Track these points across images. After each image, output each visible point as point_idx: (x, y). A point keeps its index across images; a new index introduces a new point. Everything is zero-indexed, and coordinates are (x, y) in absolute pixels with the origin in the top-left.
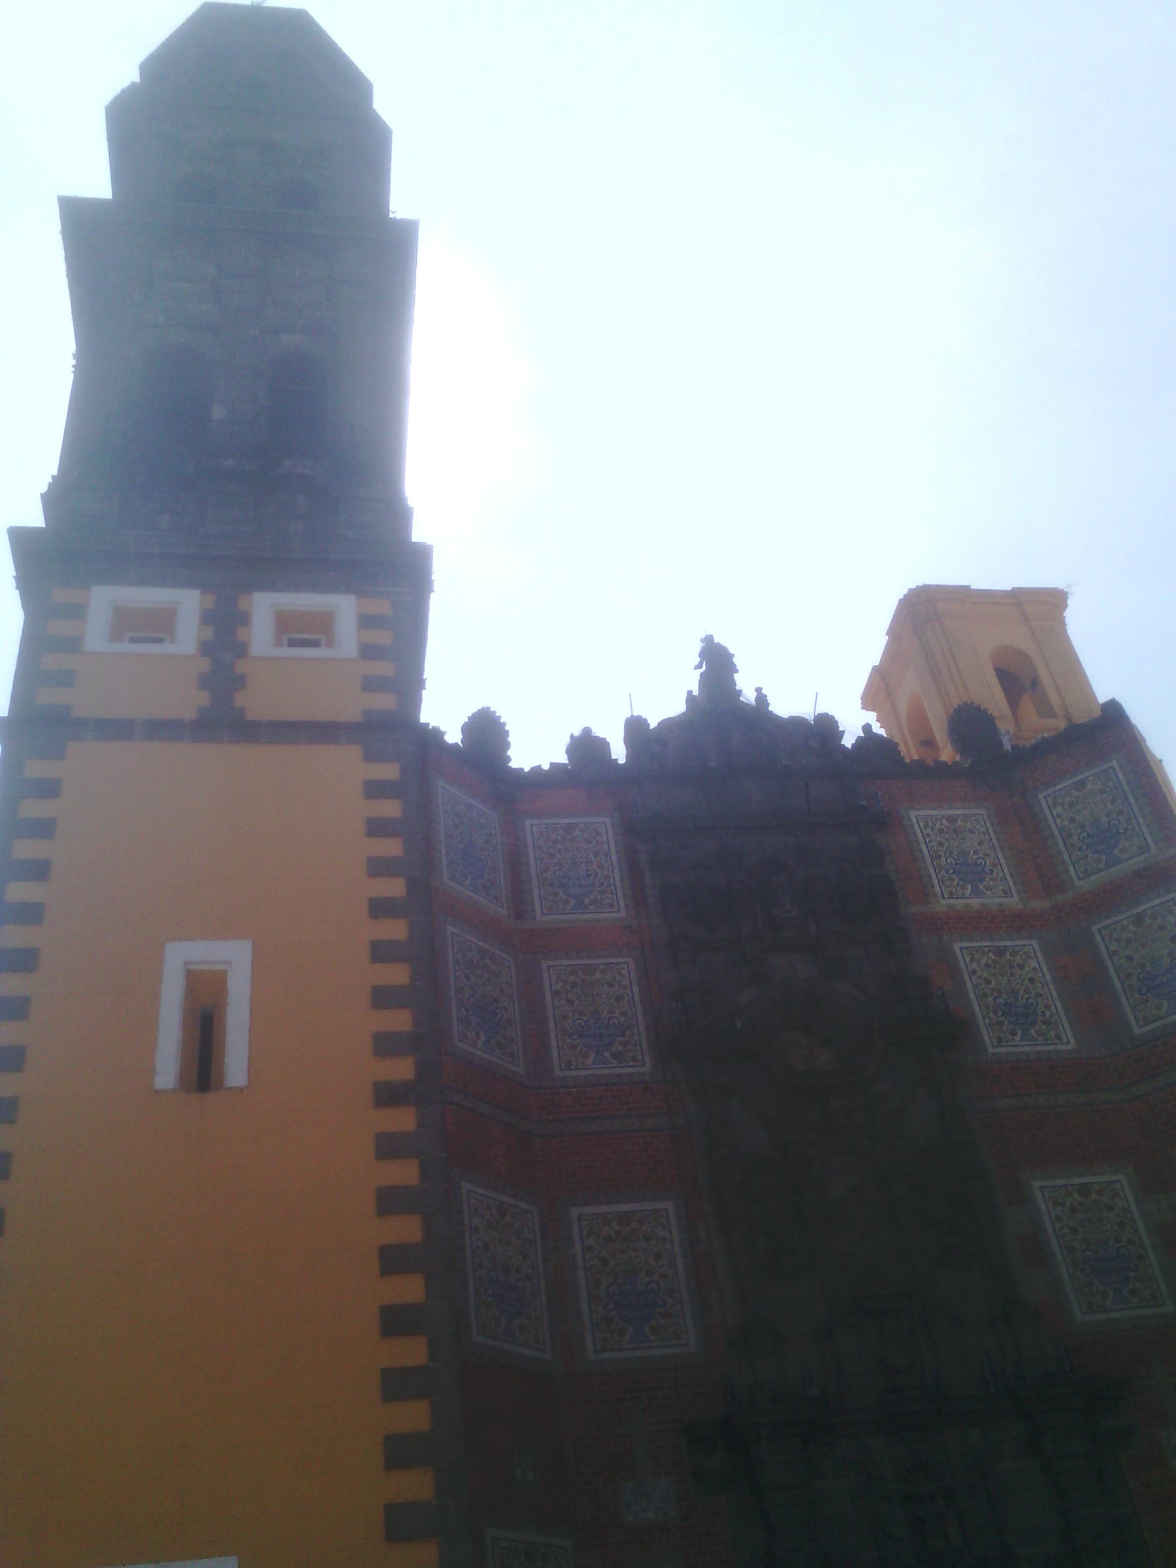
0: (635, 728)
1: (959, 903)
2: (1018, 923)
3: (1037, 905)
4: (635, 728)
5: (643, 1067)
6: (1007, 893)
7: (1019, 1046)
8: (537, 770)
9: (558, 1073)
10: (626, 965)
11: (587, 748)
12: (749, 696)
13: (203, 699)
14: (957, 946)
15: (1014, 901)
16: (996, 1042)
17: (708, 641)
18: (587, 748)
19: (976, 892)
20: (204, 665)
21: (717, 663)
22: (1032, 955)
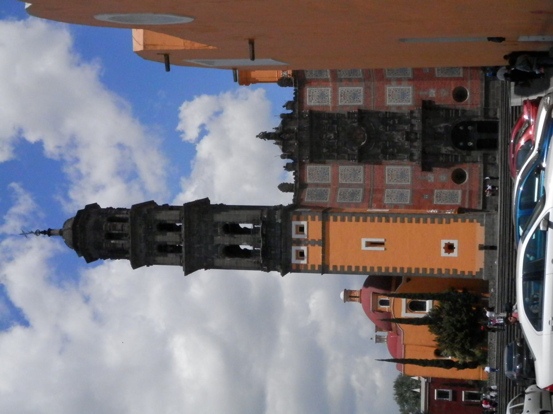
0: (283, 157)
1: (330, 100)
2: (335, 90)
3: (331, 85)
4: (283, 157)
5: (361, 167)
6: (328, 90)
7: (361, 98)
8: (295, 178)
9: (362, 182)
10: (341, 168)
11: (288, 167)
12: (274, 131)
13: (317, 246)
14: (340, 104)
15: (330, 89)
16: (360, 102)
17: (257, 136)
18: (288, 167)
19: (328, 96)
20: (309, 246)
21: (265, 136)
22: (341, 90)
